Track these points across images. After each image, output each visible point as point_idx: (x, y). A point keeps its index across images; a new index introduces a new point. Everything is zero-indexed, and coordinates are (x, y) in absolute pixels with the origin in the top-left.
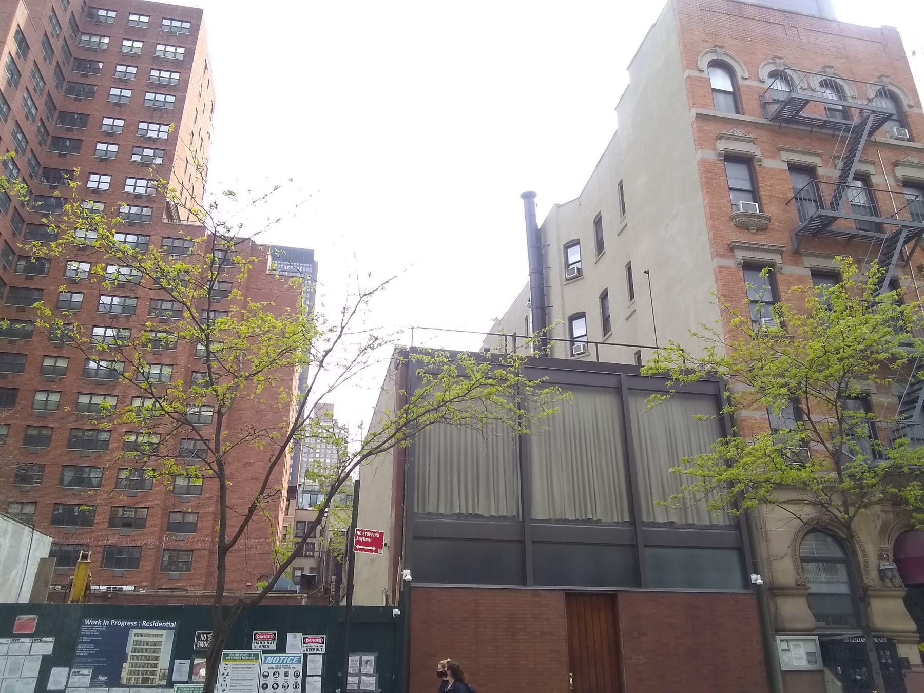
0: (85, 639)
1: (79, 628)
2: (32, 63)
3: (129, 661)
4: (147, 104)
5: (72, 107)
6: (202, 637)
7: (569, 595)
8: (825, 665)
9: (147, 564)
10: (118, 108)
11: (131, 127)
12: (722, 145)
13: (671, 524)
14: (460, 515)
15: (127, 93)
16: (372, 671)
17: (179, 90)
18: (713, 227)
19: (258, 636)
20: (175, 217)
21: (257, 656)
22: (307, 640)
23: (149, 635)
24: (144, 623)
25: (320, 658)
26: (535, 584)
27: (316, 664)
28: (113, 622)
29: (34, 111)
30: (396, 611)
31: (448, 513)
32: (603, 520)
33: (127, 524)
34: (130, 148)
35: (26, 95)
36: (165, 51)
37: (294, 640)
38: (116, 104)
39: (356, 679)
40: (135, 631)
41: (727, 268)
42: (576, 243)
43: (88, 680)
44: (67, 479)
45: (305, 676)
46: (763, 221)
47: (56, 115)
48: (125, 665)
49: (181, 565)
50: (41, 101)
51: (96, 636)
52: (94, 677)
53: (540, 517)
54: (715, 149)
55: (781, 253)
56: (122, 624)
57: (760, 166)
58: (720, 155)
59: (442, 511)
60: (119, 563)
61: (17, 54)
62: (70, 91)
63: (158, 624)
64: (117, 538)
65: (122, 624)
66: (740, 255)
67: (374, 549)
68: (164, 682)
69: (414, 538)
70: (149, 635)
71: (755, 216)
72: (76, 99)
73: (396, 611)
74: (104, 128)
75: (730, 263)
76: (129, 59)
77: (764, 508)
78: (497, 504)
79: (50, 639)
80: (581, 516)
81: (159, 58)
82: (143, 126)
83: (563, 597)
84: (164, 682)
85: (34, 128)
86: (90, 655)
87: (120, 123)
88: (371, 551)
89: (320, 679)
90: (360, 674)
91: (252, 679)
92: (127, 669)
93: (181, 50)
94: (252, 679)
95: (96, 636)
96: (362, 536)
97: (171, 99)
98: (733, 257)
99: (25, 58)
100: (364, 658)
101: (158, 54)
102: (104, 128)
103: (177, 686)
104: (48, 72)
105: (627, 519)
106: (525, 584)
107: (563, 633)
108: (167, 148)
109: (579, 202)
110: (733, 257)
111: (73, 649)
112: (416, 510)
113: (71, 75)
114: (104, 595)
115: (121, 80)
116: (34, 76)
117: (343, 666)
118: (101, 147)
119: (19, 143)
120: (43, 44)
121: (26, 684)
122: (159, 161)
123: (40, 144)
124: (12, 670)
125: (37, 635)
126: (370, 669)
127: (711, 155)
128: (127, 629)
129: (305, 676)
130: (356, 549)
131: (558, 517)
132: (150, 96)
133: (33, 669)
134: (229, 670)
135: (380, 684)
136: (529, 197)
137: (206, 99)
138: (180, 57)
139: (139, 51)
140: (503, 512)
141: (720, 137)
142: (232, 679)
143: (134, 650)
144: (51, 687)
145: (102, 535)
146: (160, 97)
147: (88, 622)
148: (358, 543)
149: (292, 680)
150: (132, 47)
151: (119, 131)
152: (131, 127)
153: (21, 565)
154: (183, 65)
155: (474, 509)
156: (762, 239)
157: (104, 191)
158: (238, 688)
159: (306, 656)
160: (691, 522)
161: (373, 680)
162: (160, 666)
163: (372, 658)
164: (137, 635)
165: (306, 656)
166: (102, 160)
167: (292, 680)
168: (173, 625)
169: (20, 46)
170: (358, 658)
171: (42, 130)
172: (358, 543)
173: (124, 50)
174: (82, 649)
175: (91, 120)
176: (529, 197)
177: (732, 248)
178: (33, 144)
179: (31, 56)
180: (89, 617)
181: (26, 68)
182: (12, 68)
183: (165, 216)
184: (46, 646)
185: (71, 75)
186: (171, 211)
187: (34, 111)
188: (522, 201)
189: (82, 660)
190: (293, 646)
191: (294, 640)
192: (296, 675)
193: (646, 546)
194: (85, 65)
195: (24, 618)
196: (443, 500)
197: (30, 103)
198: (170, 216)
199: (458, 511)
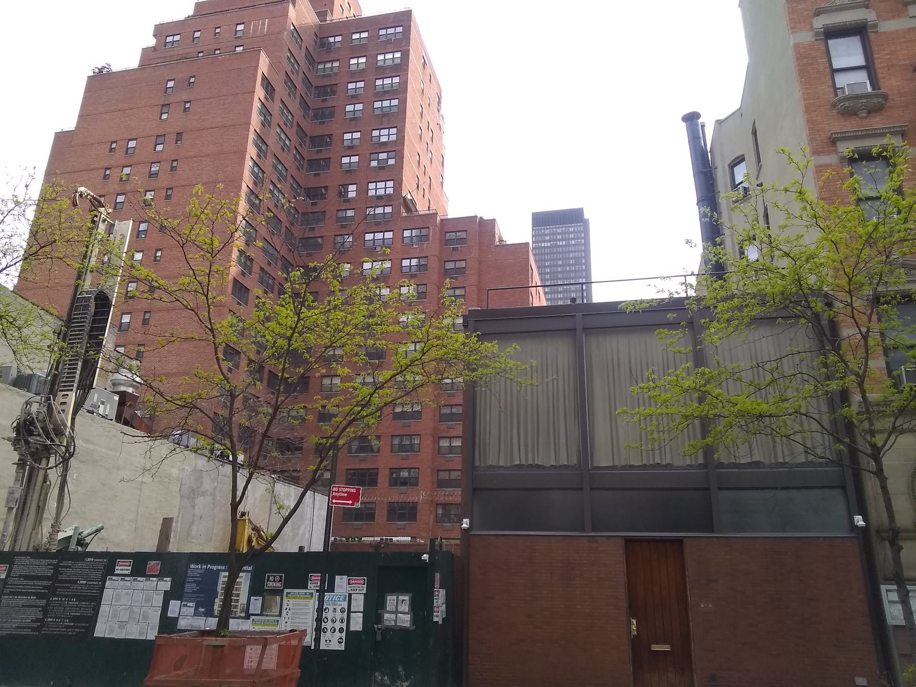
1: (186, 571)
2: (279, 102)
4: (377, 112)
5: (319, 131)
7: (628, 541)
9: (426, 517)
10: (353, 123)
11: (367, 136)
12: (820, 23)
13: (757, 464)
14: (520, 466)
15: (359, 107)
16: (407, 610)
17: (400, 92)
18: (810, 122)
19: (313, 578)
20: (413, 209)
21: (312, 594)
22: (351, 582)
25: (362, 597)
26: (594, 530)
27: (359, 602)
29: (287, 142)
30: (425, 557)
31: (509, 465)
32: (676, 464)
33: (404, 483)
34: (368, 155)
35: (278, 130)
36: (385, 60)
37: (341, 581)
38: (351, 119)
39: (393, 616)
41: (827, 166)
42: (740, 160)
43: (192, 610)
44: (354, 448)
45: (349, 612)
46: (875, 100)
47: (308, 141)
49: (452, 517)
50: (292, 132)
52: (196, 609)
53: (604, 463)
54: (812, 29)
55: (903, 135)
56: (215, 568)
57: (876, 32)
58: (817, 34)
59: (502, 464)
60: (402, 517)
61: (266, 98)
62: (316, 117)
64: (398, 495)
65: (215, 568)
66: (847, 148)
67: (350, 502)
68: (243, 615)
69: (474, 490)
71: (868, 96)
72: (321, 123)
73: (425, 557)
74: (346, 143)
75: (832, 159)
76: (357, 75)
78: (555, 453)
79: (168, 579)
80: (648, 459)
81: (381, 67)
82: (376, 133)
83: (621, 543)
84: (243, 615)
85: (290, 157)
86: (194, 592)
87: (357, 135)
88: (348, 504)
89: (361, 615)
90: (396, 612)
91: (307, 614)
93: (398, 55)
94: (307, 614)
96: (338, 492)
97: (395, 102)
98: (836, 152)
99: (273, 100)
100: (401, 598)
101: (380, 64)
102: (346, 143)
103: (252, 617)
104: (294, 105)
105: (701, 461)
106: (582, 529)
107: (622, 578)
108: (396, 148)
109: (739, 113)
110: (836, 152)
112: (477, 464)
113: (314, 102)
114: (377, 546)
115: (353, 97)
116: (283, 113)
117: (381, 604)
118: (345, 160)
119: (280, 173)
120: (286, 83)
121: (156, 611)
122: (391, 162)
123: (298, 169)
124: (147, 601)
125: (160, 576)
126: (405, 607)
127: (806, 37)
128: (219, 571)
129: (349, 612)
130: (332, 503)
131: (623, 463)
132: (377, 105)
133: (159, 600)
134: (291, 606)
135: (414, 621)
136: (691, 119)
137: (431, 93)
138: (398, 61)
139: (363, 66)
140: (564, 461)
141: (818, 13)
142: (293, 613)
144: (170, 614)
145: (383, 495)
146: (386, 103)
147: (192, 566)
148: (334, 497)
149: (339, 615)
150: (358, 64)
151: (356, 143)
152: (367, 136)
153: (307, 522)
154: (400, 69)
155: (534, 461)
156: (877, 122)
157: (353, 198)
158: (297, 620)
159: (350, 595)
160: (781, 460)
161: (408, 617)
162: (240, 602)
163: (407, 598)
165: (350, 595)
166: (347, 171)
167: (339, 615)
168: (250, 568)
169: (267, 91)
170: (395, 597)
171: (298, 157)
172: (334, 497)
173: (353, 68)
174: (189, 587)
175: (335, 138)
176: (691, 119)
177: (833, 141)
178: (293, 171)
179: (277, 97)
181: (275, 108)
182: (264, 111)
183: (403, 210)
184: (166, 584)
185: (314, 102)
186: (409, 205)
187: (287, 142)
188: (683, 125)
189: (190, 595)
190: (341, 586)
191: (341, 581)
192: (342, 611)
193: (720, 489)
194: (326, 90)
195: (152, 563)
196: (502, 452)
197: (283, 136)
198: (408, 210)
199: (517, 462)
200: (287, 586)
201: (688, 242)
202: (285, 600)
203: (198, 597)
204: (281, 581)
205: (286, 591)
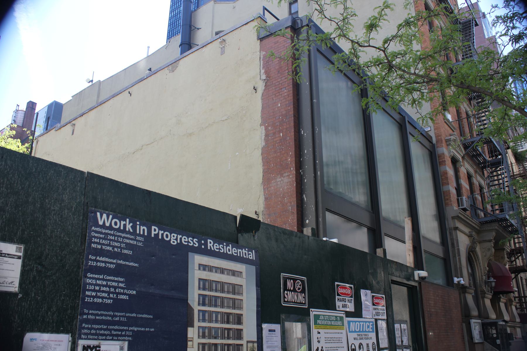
0: (102, 262)
3: (196, 324)
6: (289, 284)
8: (485, 340)
23: (222, 271)
24: (210, 243)
28: (155, 230)
40: (198, 259)
48: (192, 333)
51: (126, 257)
56: (173, 238)
63: (230, 250)
65: (173, 238)
70: (222, 271)
77: (386, 237)
86: (118, 305)
92: (197, 341)
95: (126, 257)
111: (76, 288)
128: (183, 251)
143: (203, 300)
147: (103, 219)
164: (203, 267)
174: (100, 288)
180: (105, 209)
189: (106, 315)
200: (313, 304)
201: (149, 47)
202: (314, 331)
203: (131, 322)
204: (303, 291)
205: (314, 312)
